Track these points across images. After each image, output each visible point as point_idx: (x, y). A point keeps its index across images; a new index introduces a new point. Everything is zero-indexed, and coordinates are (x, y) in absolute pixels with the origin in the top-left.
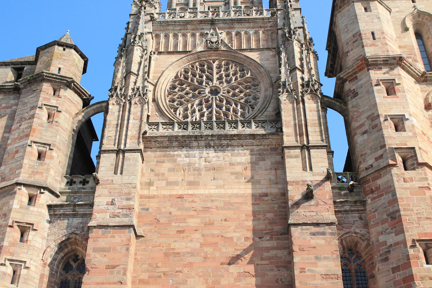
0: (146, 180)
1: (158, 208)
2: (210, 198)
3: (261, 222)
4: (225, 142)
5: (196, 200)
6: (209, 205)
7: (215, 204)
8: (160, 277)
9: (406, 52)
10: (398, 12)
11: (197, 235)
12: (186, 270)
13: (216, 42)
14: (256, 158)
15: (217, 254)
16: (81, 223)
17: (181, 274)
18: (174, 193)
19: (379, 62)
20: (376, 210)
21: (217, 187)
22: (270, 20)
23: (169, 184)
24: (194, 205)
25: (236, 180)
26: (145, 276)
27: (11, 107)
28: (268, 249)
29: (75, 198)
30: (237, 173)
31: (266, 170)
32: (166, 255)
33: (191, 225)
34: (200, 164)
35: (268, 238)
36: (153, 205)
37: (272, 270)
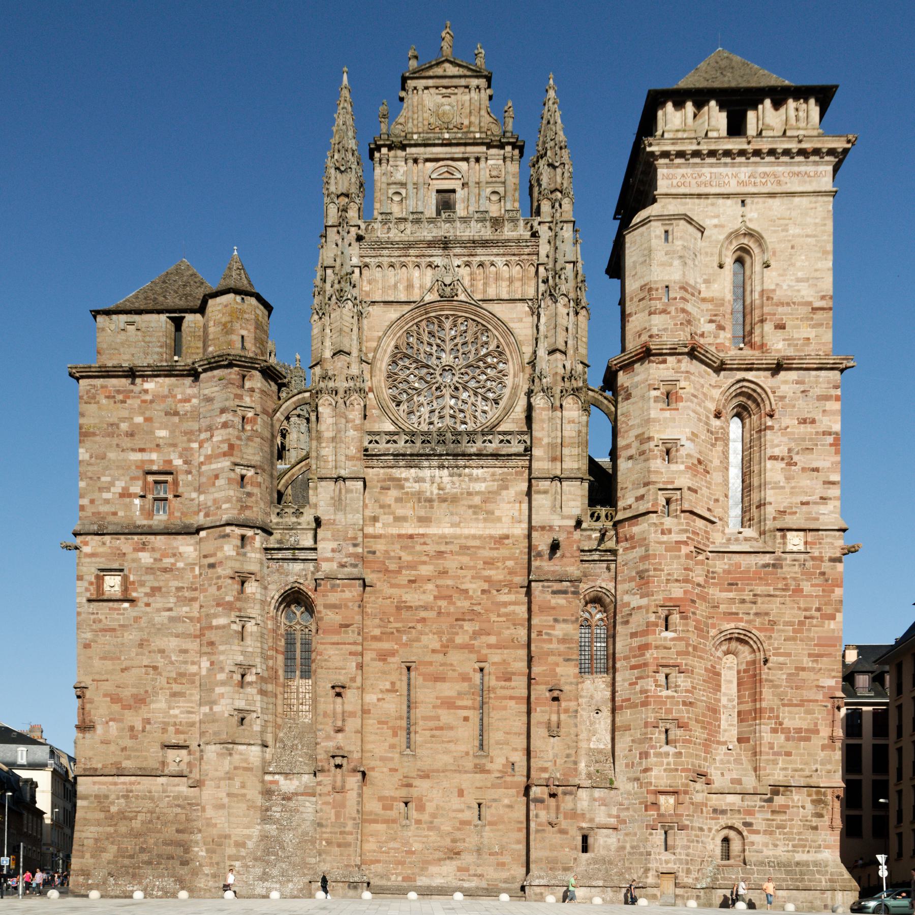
0: (368, 513)
1: (387, 552)
2: (444, 539)
3: (500, 571)
4: (461, 463)
5: (428, 541)
6: (443, 548)
7: (448, 548)
8: (392, 633)
9: (711, 310)
10: (716, 226)
11: (430, 586)
12: (419, 626)
13: (450, 285)
14: (498, 486)
15: (452, 609)
16: (303, 570)
17: (413, 631)
18: (403, 532)
19: (664, 351)
20: (626, 564)
21: (453, 525)
22: (529, 244)
23: (398, 519)
24: (425, 548)
25: (474, 517)
26: (377, 632)
27: (189, 401)
28: (505, 604)
29: (291, 536)
30: (475, 507)
31: (509, 503)
32: (398, 608)
33: (424, 573)
34: (432, 493)
35: (506, 591)
36: (380, 546)
37: (508, 628)
